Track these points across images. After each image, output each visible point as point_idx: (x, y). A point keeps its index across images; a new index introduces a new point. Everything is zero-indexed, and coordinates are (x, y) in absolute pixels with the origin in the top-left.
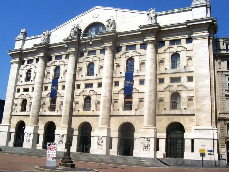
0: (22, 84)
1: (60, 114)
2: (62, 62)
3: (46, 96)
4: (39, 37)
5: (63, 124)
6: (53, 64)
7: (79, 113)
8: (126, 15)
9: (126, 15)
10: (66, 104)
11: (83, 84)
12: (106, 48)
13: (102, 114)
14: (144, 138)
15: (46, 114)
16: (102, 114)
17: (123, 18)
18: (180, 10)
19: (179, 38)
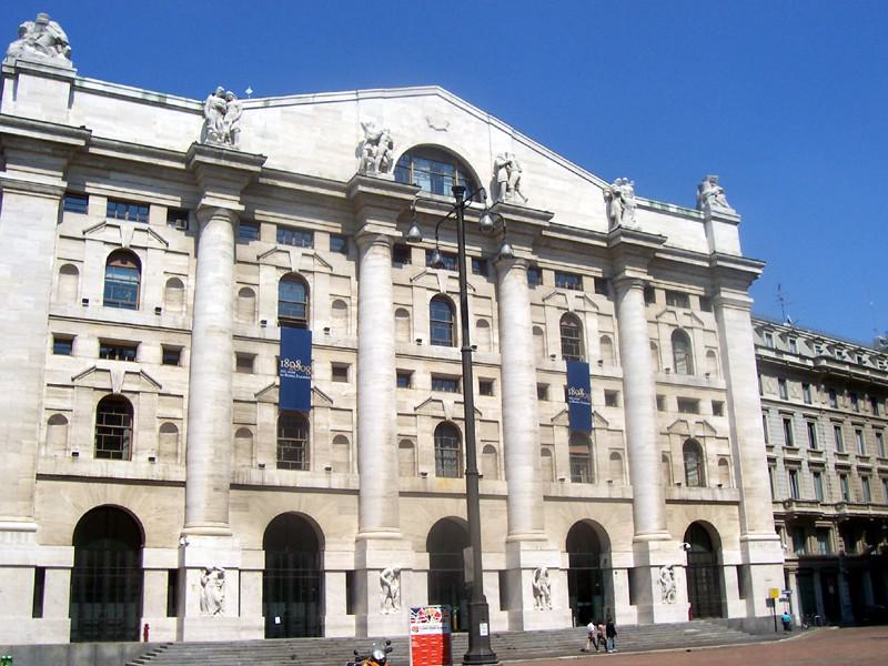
0: (90, 313)
1: (343, 481)
2: (316, 261)
3: (253, 399)
4: (169, 101)
5: (384, 525)
6: (270, 259)
7: (425, 483)
8: (541, 164)
9: (541, 164)
10: (389, 446)
11: (425, 372)
12: (518, 262)
13: (533, 492)
14: (661, 567)
15: (268, 482)
16: (533, 492)
17: (534, 172)
18: (680, 212)
19: (687, 290)
